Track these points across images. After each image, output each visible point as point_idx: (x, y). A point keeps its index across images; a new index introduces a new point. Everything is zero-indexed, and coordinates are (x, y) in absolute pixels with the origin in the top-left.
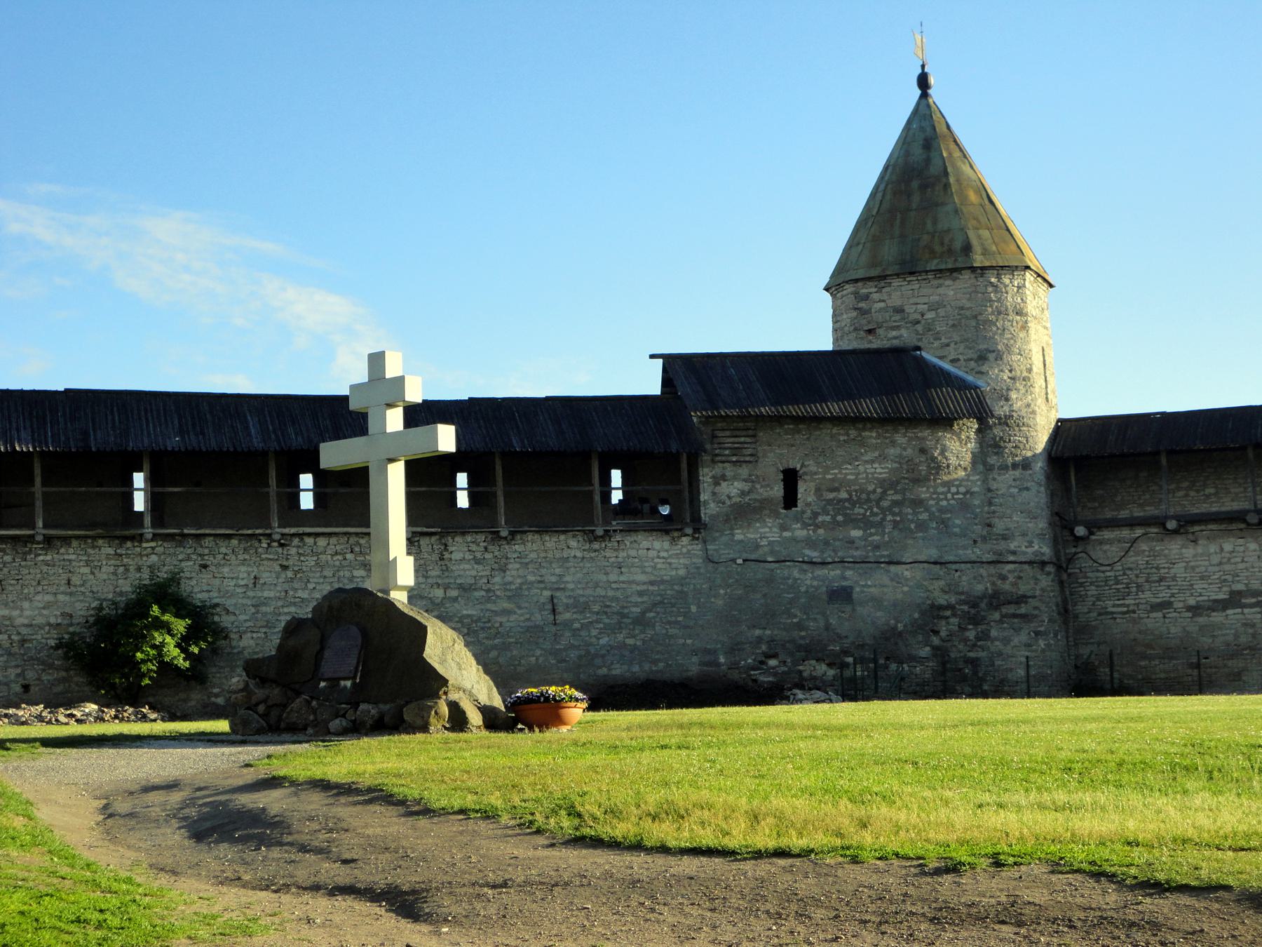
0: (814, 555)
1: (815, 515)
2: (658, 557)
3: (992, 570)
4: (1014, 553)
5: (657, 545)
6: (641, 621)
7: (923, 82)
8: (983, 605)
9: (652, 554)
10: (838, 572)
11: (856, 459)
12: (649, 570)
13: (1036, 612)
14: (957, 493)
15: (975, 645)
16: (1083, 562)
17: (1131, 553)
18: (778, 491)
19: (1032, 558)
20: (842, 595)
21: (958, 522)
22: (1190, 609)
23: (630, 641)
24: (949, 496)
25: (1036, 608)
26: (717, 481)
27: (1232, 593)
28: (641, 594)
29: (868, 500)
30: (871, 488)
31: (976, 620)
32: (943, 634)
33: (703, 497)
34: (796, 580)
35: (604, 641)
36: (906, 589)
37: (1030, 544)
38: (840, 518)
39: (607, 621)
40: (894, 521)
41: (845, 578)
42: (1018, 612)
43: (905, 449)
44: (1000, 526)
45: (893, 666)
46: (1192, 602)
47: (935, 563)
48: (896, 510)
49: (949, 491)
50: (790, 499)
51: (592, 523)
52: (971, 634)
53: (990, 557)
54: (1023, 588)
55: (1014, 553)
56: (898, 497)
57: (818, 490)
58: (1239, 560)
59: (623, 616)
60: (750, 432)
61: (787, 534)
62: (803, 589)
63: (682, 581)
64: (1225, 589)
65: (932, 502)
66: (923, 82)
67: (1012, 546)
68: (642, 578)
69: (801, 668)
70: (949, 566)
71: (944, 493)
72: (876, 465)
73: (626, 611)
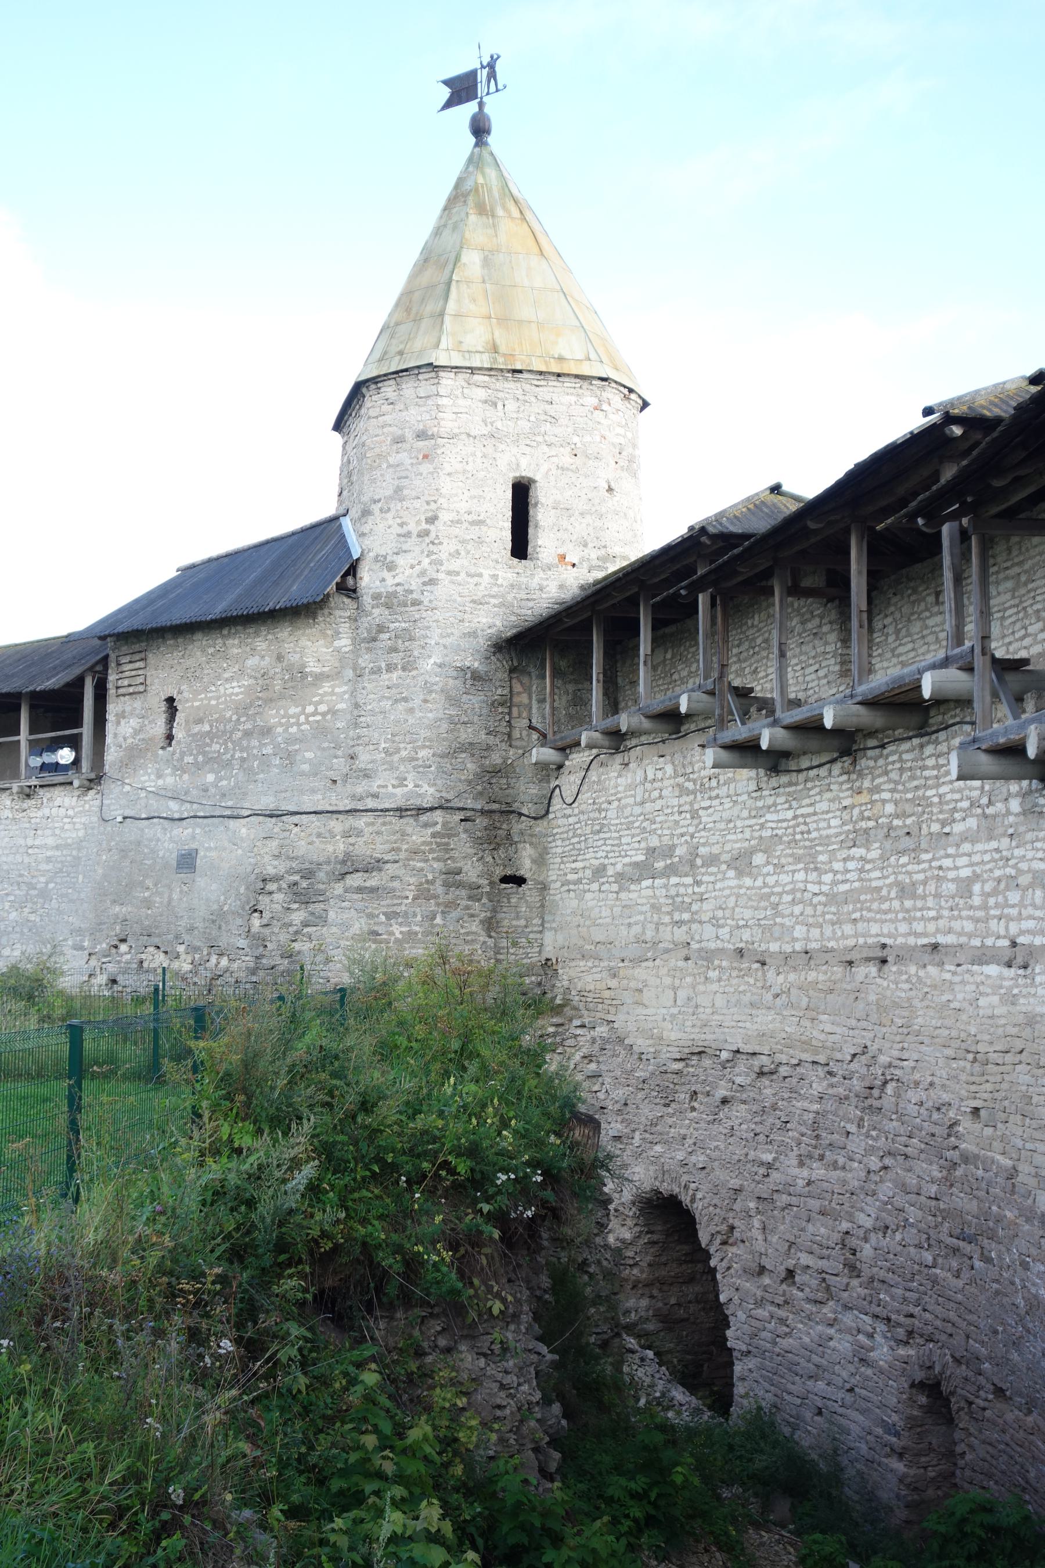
0: (174, 808)
1: (183, 754)
2: (67, 817)
3: (350, 821)
4: (375, 796)
5: (67, 800)
6: (44, 894)
7: (480, 129)
8: (321, 875)
9: (62, 811)
10: (190, 830)
11: (219, 678)
12: (57, 832)
13: (396, 884)
14: (313, 714)
15: (296, 933)
16: (557, 804)
17: (585, 787)
18: (159, 727)
19: (401, 803)
20: (187, 862)
21: (309, 755)
22: (620, 876)
23: (32, 917)
24: (302, 719)
25: (393, 878)
26: (121, 716)
27: (651, 851)
28: (49, 860)
29: (224, 732)
30: (228, 714)
31: (302, 896)
32: (267, 915)
33: (109, 740)
34: (158, 840)
35: (13, 915)
36: (240, 852)
37: (402, 781)
38: (200, 758)
39: (17, 892)
40: (243, 760)
41: (193, 837)
42: (368, 884)
43: (263, 657)
44: (364, 758)
45: (214, 959)
46: (619, 867)
47: (271, 816)
48: (245, 743)
49: (303, 712)
50: (170, 738)
51: (16, 775)
52: (298, 917)
53: (346, 804)
54: (380, 849)
55: (375, 796)
56: (248, 726)
57: (187, 722)
58: (656, 794)
59: (31, 886)
60: (142, 655)
61: (160, 782)
62: (161, 854)
63: (79, 844)
64: (643, 845)
65: (280, 730)
66: (480, 129)
67: (374, 786)
68: (51, 841)
69: (143, 956)
70: (284, 818)
71: (297, 716)
72: (235, 684)
73: (34, 881)
